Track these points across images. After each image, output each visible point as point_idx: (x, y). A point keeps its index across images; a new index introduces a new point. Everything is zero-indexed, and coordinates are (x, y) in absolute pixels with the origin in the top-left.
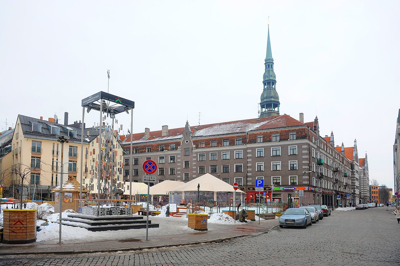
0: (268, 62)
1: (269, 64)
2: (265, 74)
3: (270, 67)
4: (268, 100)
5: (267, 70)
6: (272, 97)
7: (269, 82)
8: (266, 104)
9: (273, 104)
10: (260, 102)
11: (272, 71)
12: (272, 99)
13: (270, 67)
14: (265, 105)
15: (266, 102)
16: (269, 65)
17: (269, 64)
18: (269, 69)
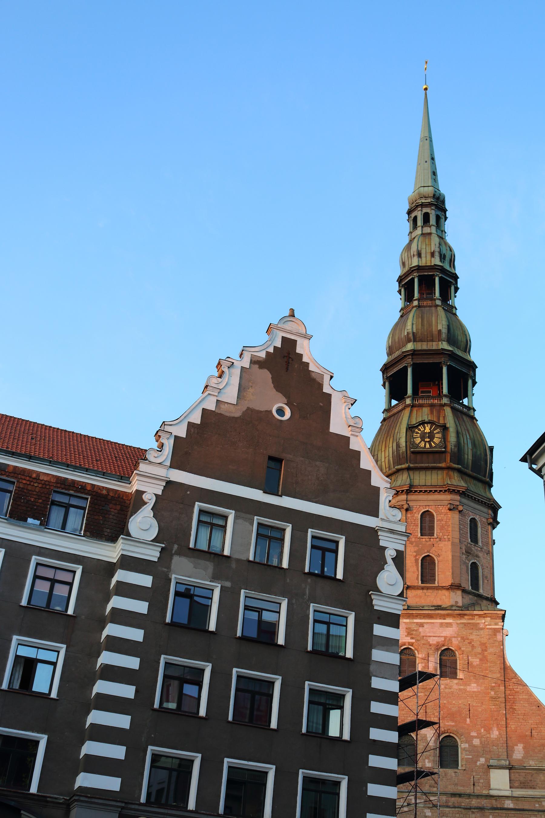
0: (423, 205)
2: (408, 247)
3: (433, 221)
5: (419, 231)
8: (415, 367)
10: (384, 359)
11: (441, 238)
12: (445, 346)
13: (433, 221)
14: (410, 371)
15: (414, 353)
18: (427, 230)
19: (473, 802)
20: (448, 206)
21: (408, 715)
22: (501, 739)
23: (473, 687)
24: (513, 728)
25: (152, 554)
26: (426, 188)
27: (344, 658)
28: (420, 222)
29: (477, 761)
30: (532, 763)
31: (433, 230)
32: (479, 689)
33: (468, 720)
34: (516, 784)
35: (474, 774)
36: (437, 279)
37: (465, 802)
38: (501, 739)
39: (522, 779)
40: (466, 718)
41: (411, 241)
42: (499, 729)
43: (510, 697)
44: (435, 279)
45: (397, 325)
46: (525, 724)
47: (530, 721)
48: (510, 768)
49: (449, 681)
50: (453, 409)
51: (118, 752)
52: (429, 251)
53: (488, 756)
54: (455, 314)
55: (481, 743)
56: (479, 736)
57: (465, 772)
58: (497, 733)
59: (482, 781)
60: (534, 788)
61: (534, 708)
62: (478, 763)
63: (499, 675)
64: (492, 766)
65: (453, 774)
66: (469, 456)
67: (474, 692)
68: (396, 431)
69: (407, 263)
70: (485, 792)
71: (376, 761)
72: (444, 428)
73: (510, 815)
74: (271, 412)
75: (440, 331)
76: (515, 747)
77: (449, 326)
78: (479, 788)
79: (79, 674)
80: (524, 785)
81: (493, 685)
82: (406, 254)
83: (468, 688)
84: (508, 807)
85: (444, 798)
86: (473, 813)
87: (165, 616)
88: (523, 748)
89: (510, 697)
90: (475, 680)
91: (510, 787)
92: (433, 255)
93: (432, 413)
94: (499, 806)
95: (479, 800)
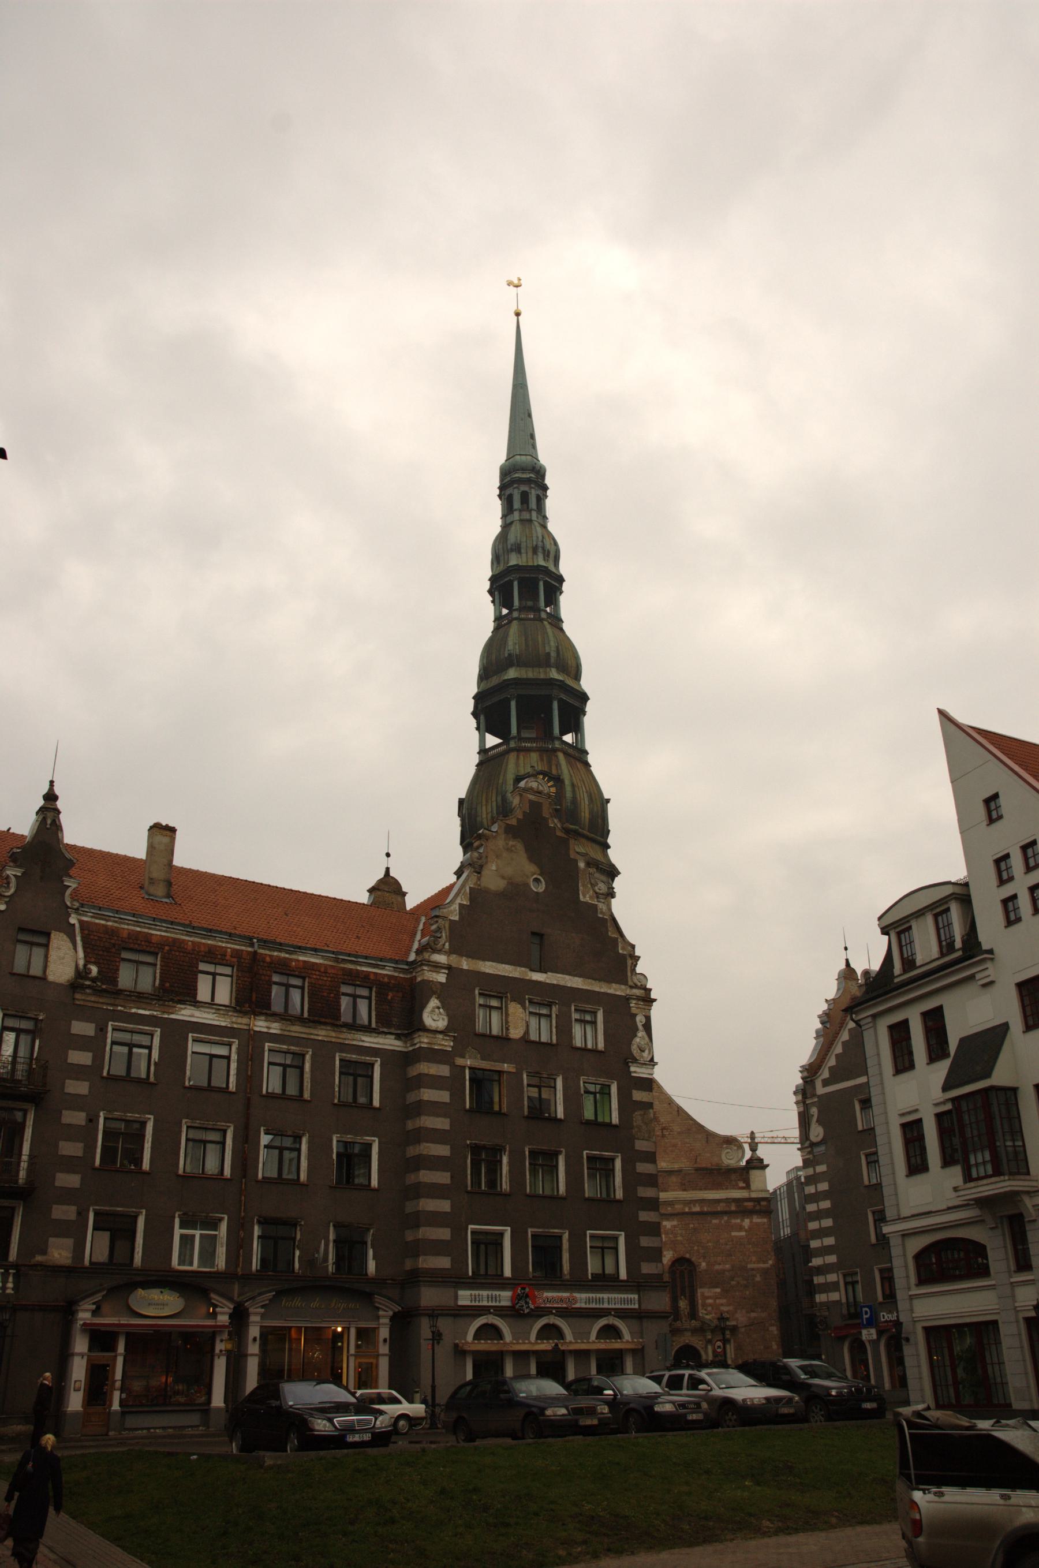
0: (520, 481)
1: (523, 485)
3: (533, 504)
4: (529, 674)
5: (516, 516)
6: (545, 662)
7: (526, 580)
8: (520, 700)
9: (555, 705)
11: (544, 527)
12: (554, 674)
13: (533, 504)
14: (513, 704)
15: (516, 682)
16: (525, 498)
17: (523, 485)
18: (526, 515)
20: (548, 481)
25: (446, 1044)
26: (524, 458)
27: (610, 1125)
28: (517, 504)
31: (534, 514)
36: (541, 584)
41: (506, 527)
44: (538, 584)
45: (491, 639)
50: (565, 753)
51: (444, 1234)
52: (530, 545)
54: (562, 630)
66: (585, 814)
68: (501, 781)
69: (502, 558)
71: (644, 1216)
72: (558, 780)
74: (527, 885)
75: (549, 654)
77: (557, 647)
79: (402, 1165)
82: (501, 547)
87: (465, 1103)
92: (535, 550)
93: (542, 760)
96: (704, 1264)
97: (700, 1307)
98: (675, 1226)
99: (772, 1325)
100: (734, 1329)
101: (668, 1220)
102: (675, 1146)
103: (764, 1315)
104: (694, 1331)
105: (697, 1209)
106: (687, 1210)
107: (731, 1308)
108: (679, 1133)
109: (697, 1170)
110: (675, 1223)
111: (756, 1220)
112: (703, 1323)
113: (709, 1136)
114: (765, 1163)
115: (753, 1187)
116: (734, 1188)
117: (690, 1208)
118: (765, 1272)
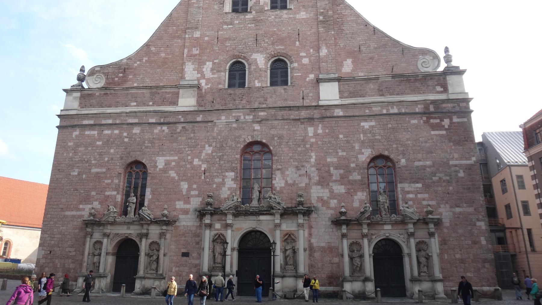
19: (302, 114)
21: (239, 44)
22: (330, 56)
23: (303, 15)
24: (342, 46)
29: (307, 77)
30: (360, 74)
32: (308, 16)
33: (297, 43)
34: (346, 94)
35: (304, 89)
37: (294, 114)
38: (330, 56)
39: (351, 89)
40: (296, 41)
42: (327, 47)
43: (338, 20)
46: (354, 41)
47: (358, 39)
48: (339, 80)
49: (279, 12)
53: (317, 73)
55: (310, 61)
56: (308, 56)
57: (294, 88)
58: (326, 51)
59: (311, 94)
60: (364, 97)
61: (363, 27)
62: (307, 79)
63: (327, 2)
64: (321, 79)
65: (283, 91)
67: (303, 19)
70: (314, 104)
73: (340, 122)
76: (344, 62)
78: (308, 101)
80: (353, 95)
81: (322, 11)
83: (298, 16)
84: (338, 115)
85: (273, 112)
86: (302, 123)
88: (352, 62)
89: (338, 20)
90: (304, 9)
91: (340, 98)
94: (328, 115)
95: (308, 111)
96: (403, 161)
97: (401, 202)
98: (372, 127)
99: (478, 220)
100: (438, 223)
101: (366, 121)
102: (372, 58)
103: (471, 210)
104: (395, 223)
105: (395, 110)
106: (385, 112)
107: (433, 203)
108: (375, 48)
109: (394, 77)
110: (373, 123)
111: (455, 120)
112: (405, 216)
113: (405, 50)
114: (461, 68)
115: (450, 90)
116: (431, 92)
117: (388, 110)
118: (469, 168)
